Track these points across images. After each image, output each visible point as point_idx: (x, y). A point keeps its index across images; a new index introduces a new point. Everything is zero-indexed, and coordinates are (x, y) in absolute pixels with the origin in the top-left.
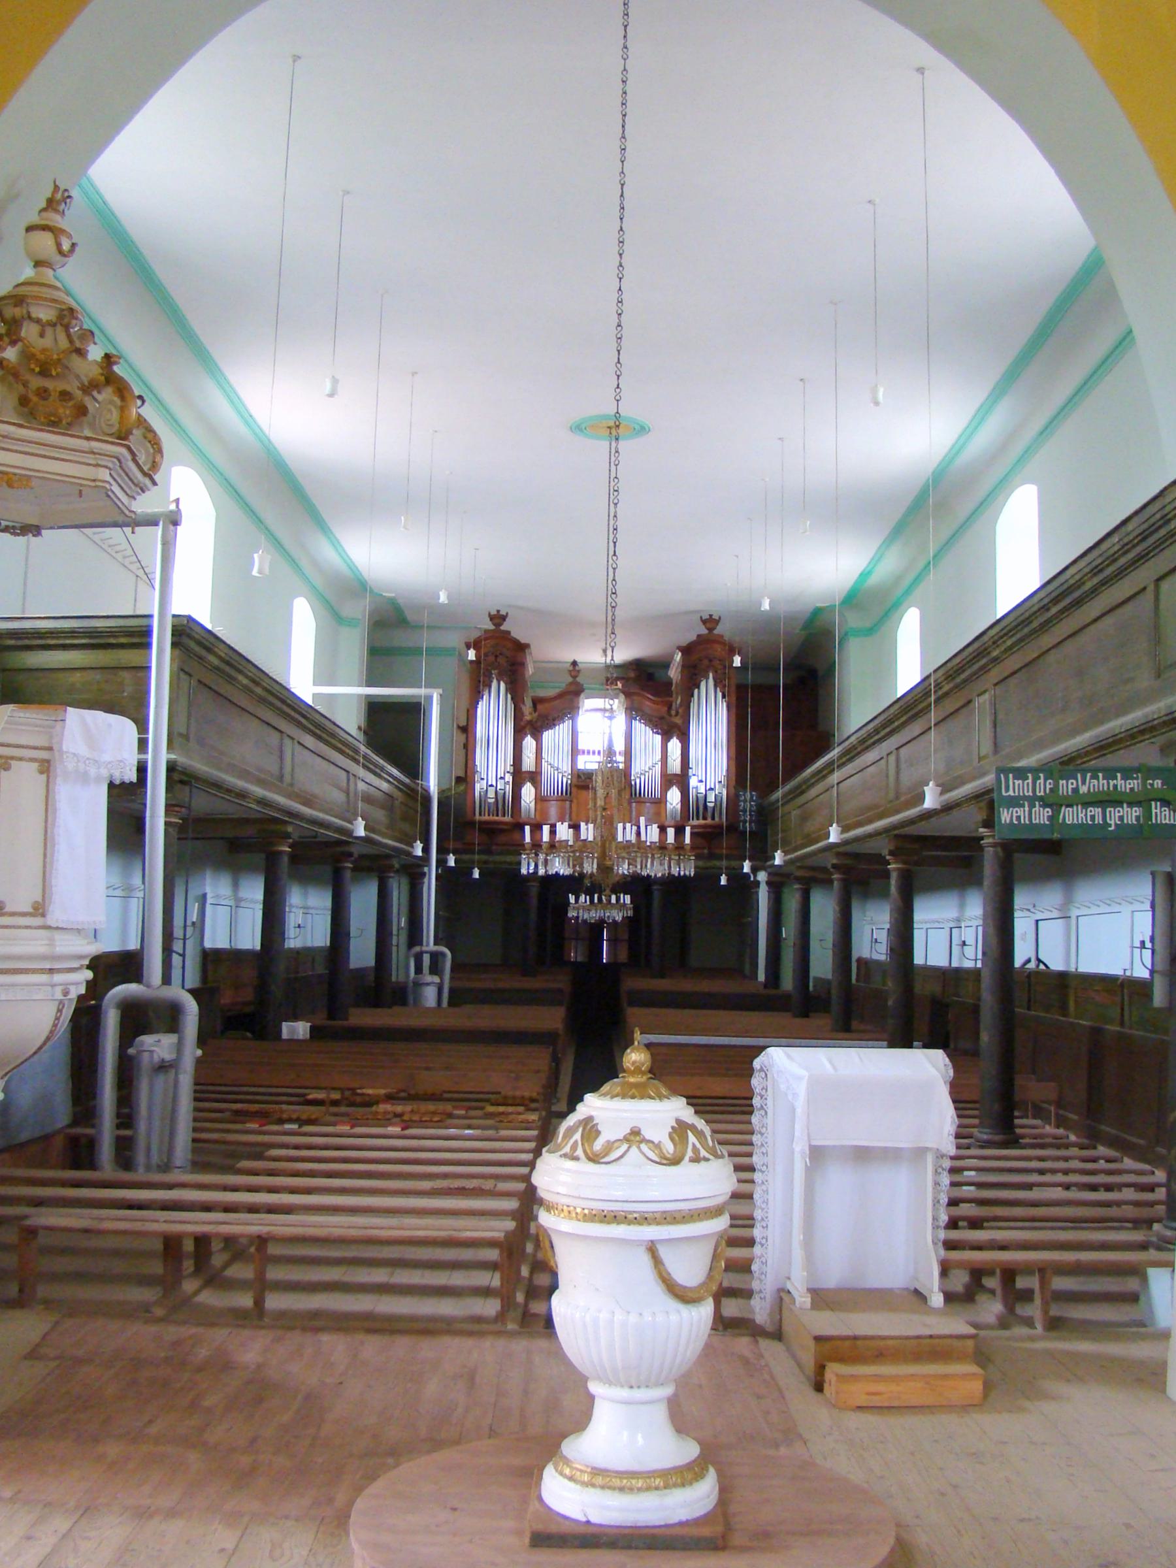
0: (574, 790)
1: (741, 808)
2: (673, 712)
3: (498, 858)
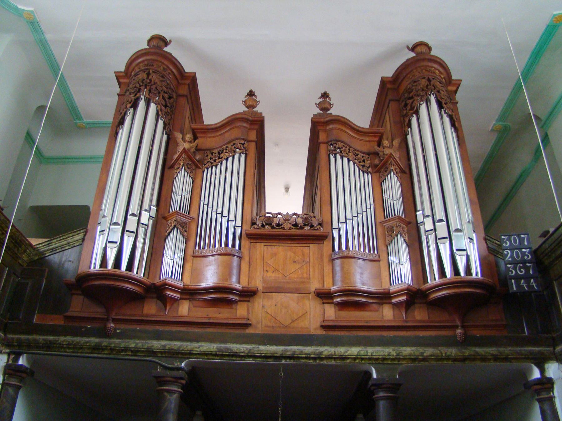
0: (245, 242)
1: (508, 258)
2: (386, 143)
3: (115, 342)
